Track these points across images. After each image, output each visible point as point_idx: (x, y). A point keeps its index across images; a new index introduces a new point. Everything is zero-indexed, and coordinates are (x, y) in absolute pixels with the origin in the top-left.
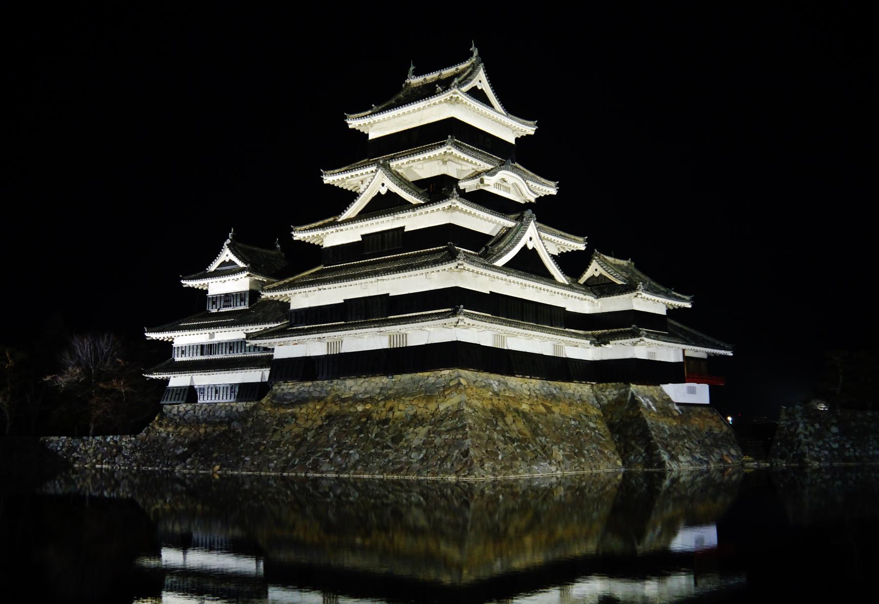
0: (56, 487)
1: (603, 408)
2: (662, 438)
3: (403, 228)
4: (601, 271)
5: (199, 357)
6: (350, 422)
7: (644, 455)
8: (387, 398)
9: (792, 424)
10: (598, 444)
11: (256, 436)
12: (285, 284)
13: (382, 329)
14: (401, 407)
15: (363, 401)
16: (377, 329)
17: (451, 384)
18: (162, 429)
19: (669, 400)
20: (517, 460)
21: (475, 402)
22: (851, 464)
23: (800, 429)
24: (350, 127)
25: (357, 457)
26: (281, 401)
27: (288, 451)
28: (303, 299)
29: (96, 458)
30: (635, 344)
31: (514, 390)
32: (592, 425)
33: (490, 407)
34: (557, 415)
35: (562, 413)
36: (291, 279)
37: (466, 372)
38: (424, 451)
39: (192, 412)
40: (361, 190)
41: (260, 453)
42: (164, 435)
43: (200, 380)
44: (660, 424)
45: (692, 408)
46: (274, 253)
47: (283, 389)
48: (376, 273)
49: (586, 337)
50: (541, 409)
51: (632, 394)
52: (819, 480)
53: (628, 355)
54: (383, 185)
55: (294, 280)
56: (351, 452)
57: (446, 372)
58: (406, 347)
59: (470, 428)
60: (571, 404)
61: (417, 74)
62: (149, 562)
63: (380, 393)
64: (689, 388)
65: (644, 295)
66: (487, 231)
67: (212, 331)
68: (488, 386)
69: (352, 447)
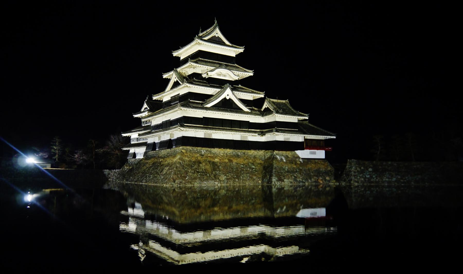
0: (106, 187)
5: (136, 142)
22: (372, 184)
52: (359, 191)
61: (202, 32)
62: (123, 212)
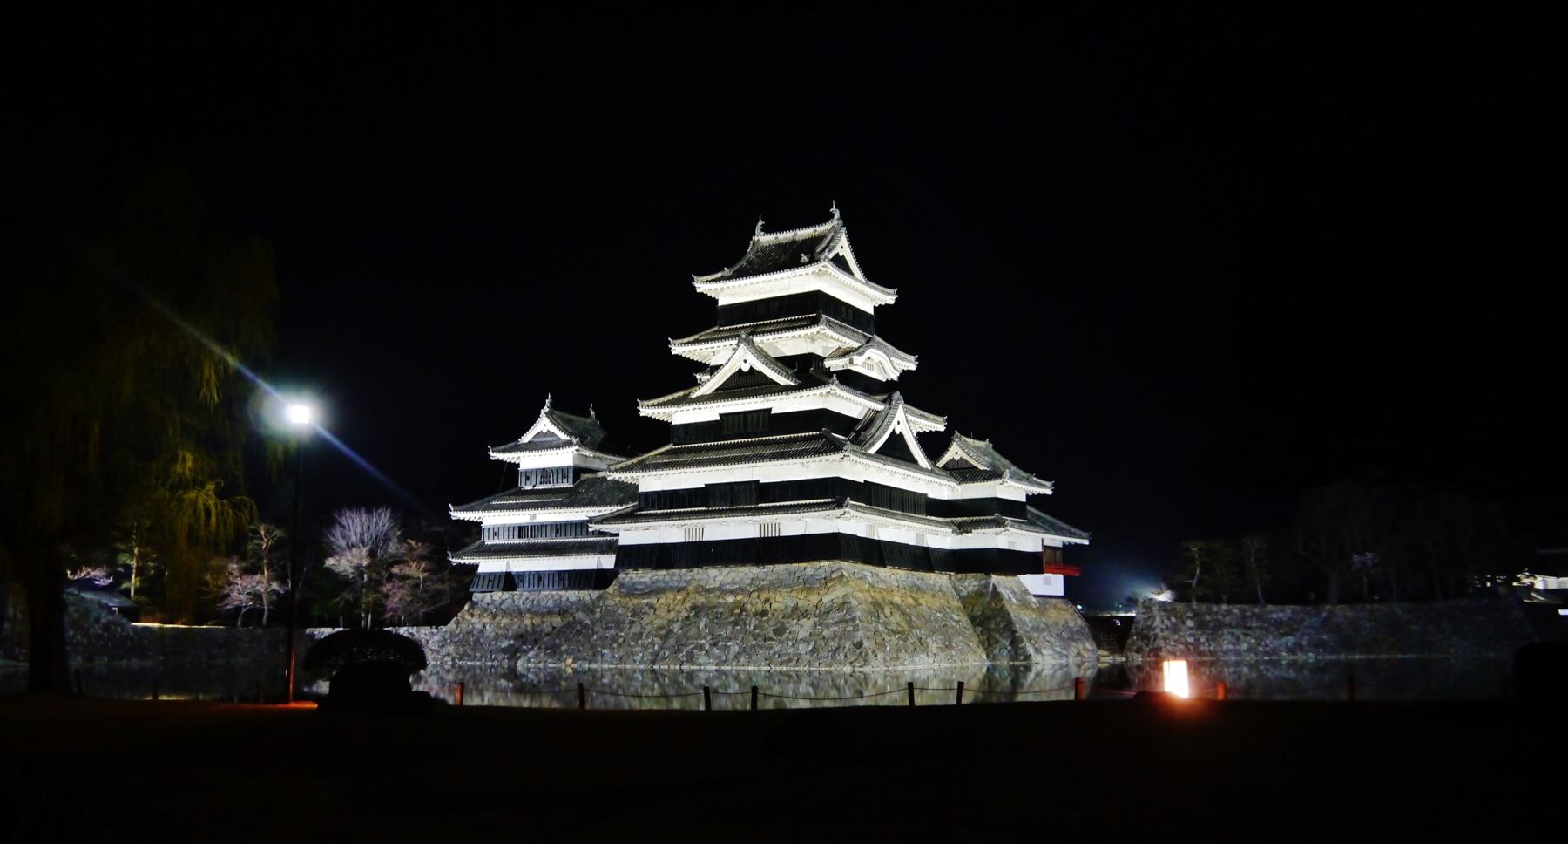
1: (963, 600)
4: (962, 454)
5: (517, 541)
8: (760, 589)
14: (779, 598)
15: (732, 592)
19: (1026, 592)
21: (860, 595)
23: (1157, 622)
26: (631, 591)
28: (652, 481)
41: (620, 645)
42: (479, 626)
43: (519, 565)
49: (948, 525)
50: (910, 601)
57: (825, 564)
61: (767, 230)
65: (1011, 483)
66: (855, 415)
67: (532, 512)
68: (863, 578)
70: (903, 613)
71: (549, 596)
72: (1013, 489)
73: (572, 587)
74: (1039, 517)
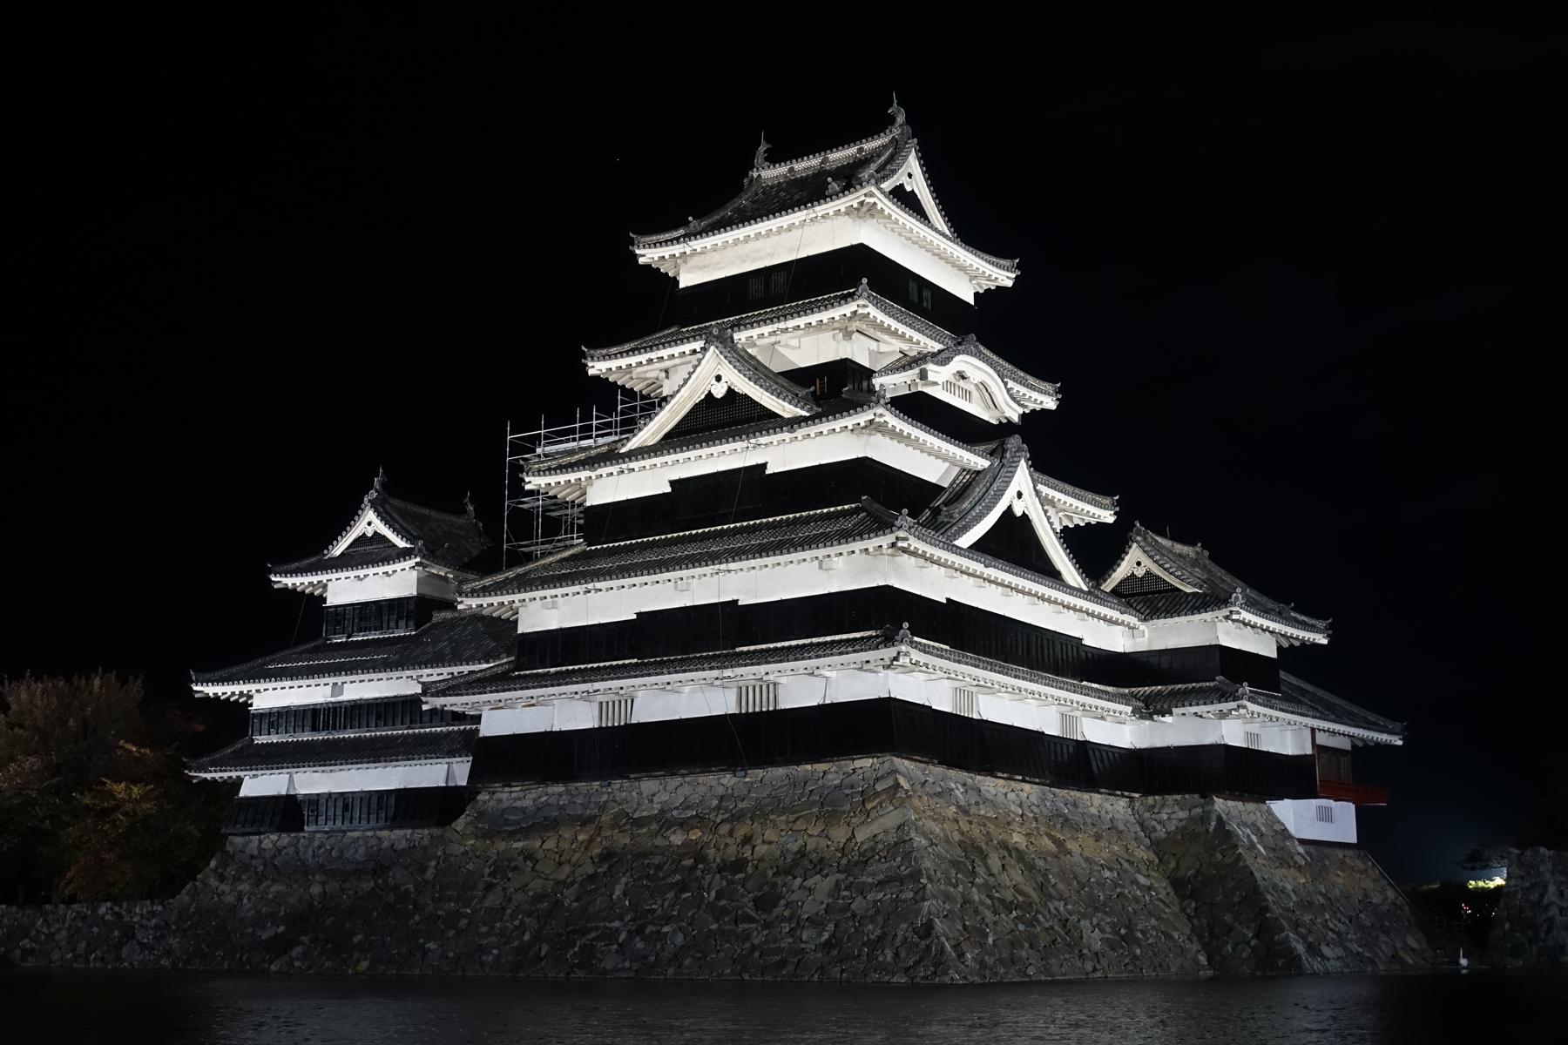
1: (1156, 845)
2: (1288, 910)
3: (764, 466)
5: (307, 737)
6: (659, 867)
7: (1253, 943)
8: (736, 818)
9: (1533, 886)
10: (1159, 918)
11: (449, 899)
12: (507, 582)
13: (728, 673)
14: (770, 834)
15: (684, 825)
16: (715, 673)
17: (879, 787)
18: (224, 887)
19: (1285, 833)
20: (1022, 947)
21: (931, 825)
24: (641, 261)
25: (680, 939)
26: (496, 826)
27: (521, 929)
28: (546, 611)
29: (73, 950)
30: (1223, 715)
31: (993, 804)
32: (1142, 880)
33: (957, 837)
34: (1077, 858)
35: (1086, 854)
36: (520, 570)
37: (906, 762)
38: (831, 927)
39: (291, 850)
40: (666, 392)
41: (460, 933)
42: (230, 899)
43: (312, 782)
44: (1277, 880)
45: (1327, 850)
46: (461, 521)
47: (501, 801)
48: (714, 558)
50: (1047, 843)
51: (1219, 818)
53: (1209, 739)
54: (718, 378)
55: (526, 574)
56: (665, 929)
57: (866, 762)
58: (775, 711)
59: (930, 879)
60: (1098, 838)
61: (774, 158)
63: (718, 808)
64: (1319, 808)
68: (946, 794)
69: (668, 919)
70: (1030, 868)
71: (364, 835)
72: (1247, 631)
73: (395, 822)
74: (1303, 692)
